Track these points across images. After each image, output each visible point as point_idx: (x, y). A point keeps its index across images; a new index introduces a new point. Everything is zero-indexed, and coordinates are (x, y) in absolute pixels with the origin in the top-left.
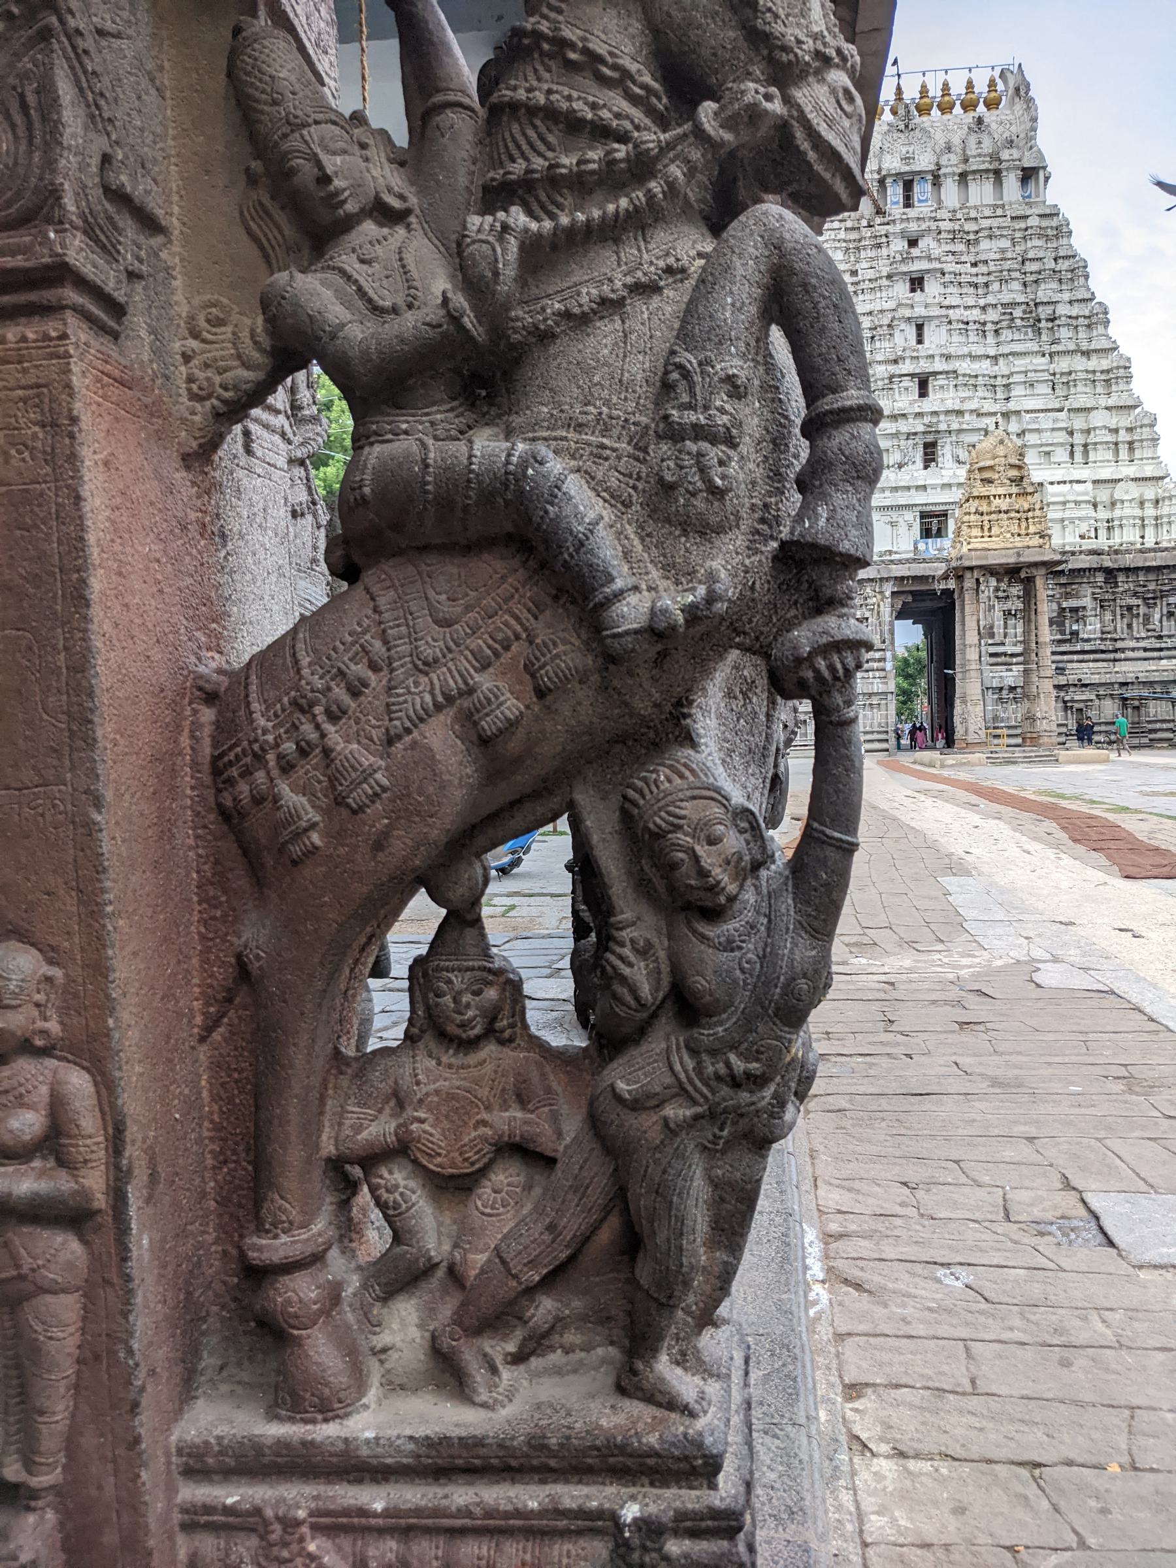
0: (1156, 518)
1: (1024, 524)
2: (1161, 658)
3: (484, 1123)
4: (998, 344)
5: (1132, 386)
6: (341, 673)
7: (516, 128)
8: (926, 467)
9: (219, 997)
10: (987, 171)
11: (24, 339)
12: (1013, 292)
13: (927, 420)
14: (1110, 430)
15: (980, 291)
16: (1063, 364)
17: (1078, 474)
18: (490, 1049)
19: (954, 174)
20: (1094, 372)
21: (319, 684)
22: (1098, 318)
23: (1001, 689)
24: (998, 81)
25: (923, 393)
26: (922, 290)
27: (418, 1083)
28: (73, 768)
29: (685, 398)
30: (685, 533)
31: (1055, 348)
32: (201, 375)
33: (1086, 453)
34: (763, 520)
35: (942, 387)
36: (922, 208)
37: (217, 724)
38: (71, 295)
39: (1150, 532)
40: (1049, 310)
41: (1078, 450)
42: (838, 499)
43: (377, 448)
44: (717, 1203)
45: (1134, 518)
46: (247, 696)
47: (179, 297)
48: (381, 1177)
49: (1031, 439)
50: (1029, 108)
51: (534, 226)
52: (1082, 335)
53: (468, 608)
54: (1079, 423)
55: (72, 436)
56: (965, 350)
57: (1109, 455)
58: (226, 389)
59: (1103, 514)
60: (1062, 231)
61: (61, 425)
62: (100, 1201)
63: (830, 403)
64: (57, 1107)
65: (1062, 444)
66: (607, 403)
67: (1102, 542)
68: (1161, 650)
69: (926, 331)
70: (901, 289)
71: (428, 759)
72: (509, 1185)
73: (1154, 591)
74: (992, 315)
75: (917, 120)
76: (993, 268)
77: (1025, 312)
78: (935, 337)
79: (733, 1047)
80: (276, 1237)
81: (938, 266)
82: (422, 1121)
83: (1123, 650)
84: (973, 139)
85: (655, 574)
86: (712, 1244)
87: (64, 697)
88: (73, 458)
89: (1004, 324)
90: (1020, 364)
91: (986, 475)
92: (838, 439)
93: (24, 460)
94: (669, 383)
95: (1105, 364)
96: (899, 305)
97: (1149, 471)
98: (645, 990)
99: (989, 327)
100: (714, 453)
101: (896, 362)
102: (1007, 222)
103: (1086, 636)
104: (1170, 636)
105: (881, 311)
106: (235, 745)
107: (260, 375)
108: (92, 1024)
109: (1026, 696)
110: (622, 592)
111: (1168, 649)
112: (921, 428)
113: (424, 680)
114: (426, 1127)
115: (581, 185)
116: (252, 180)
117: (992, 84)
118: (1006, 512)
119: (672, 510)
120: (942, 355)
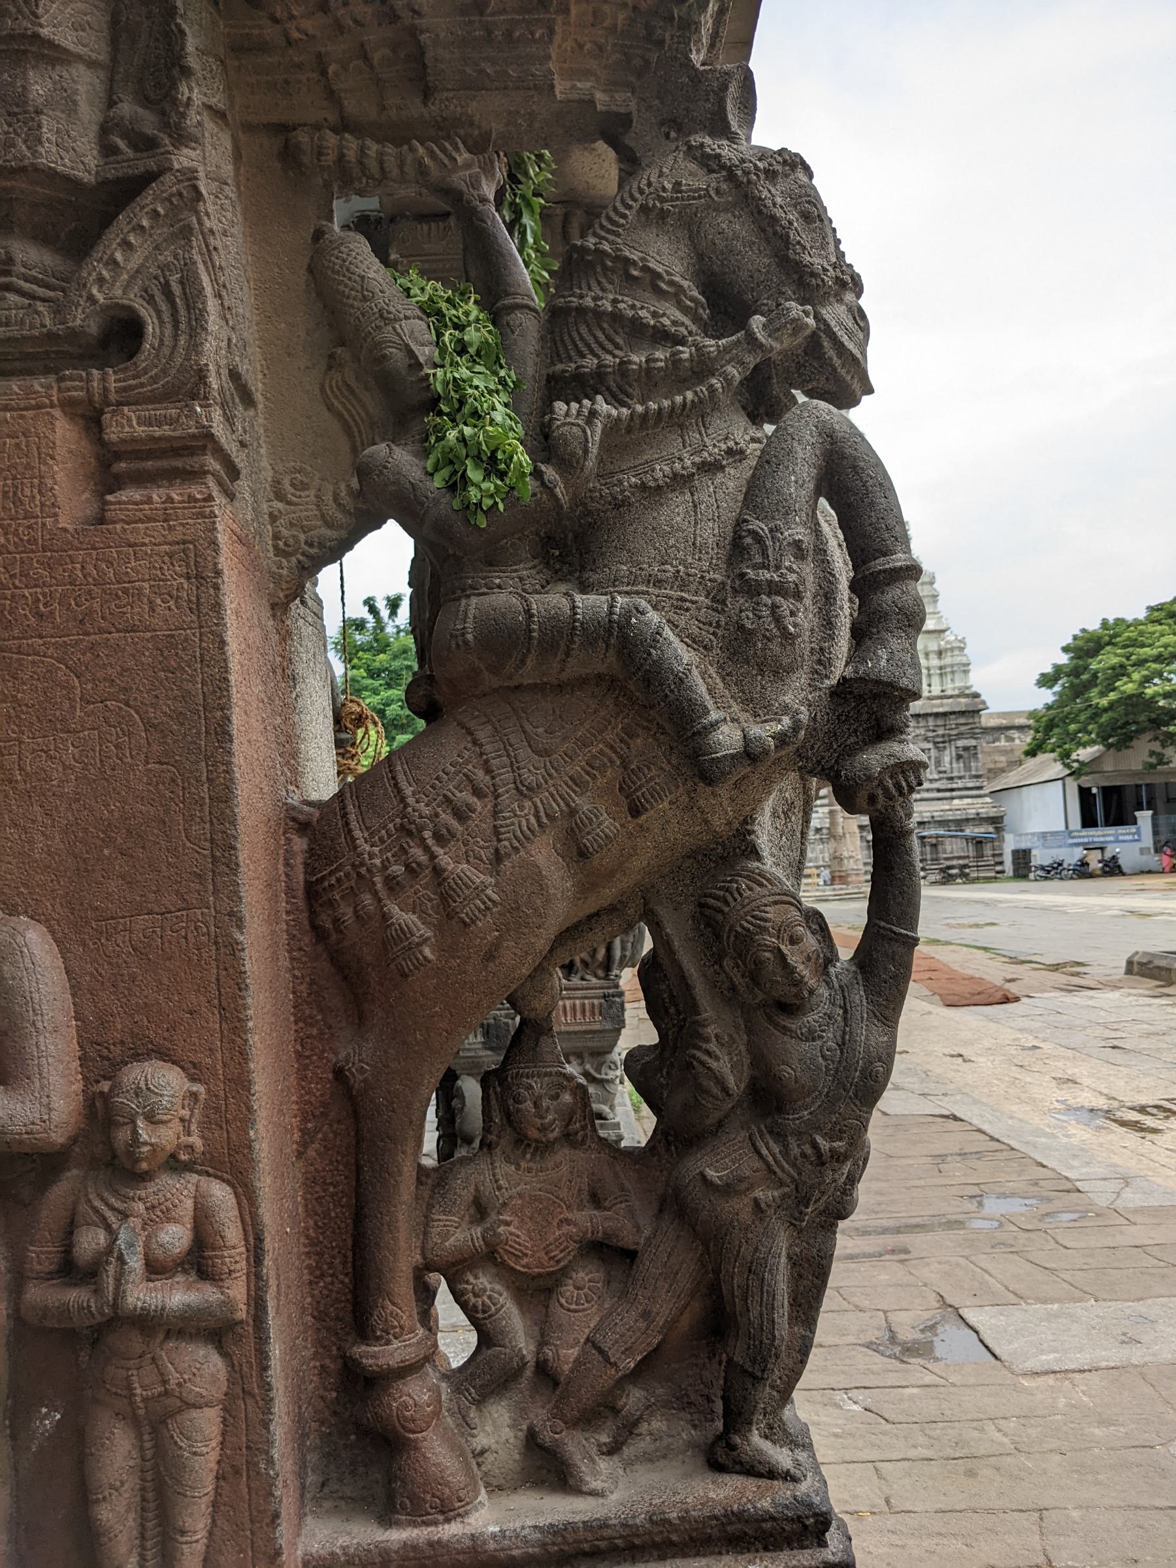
0: (941, 668)
2: (952, 798)
3: (567, 1221)
6: (448, 800)
7: (584, 330)
9: (317, 1113)
11: (170, 500)
18: (564, 1154)
21: (427, 811)
27: (499, 1188)
28: (216, 892)
29: (758, 559)
30: (761, 672)
32: (285, 532)
34: (819, 662)
37: (311, 851)
38: (213, 464)
42: (895, 644)
43: (474, 600)
44: (796, 1278)
46: (347, 824)
47: (265, 463)
48: (467, 1282)
51: (614, 412)
53: (565, 739)
55: (217, 587)
58: (311, 545)
61: (205, 577)
62: (242, 1314)
63: (880, 564)
64: (202, 1221)
66: (683, 562)
68: (952, 790)
71: (536, 876)
72: (590, 1281)
73: (943, 736)
79: (819, 1129)
80: (388, 1342)
82: (508, 1224)
85: (736, 708)
86: (793, 1320)
87: (208, 826)
88: (217, 607)
92: (892, 595)
93: (169, 609)
94: (739, 546)
98: (731, 1081)
100: (785, 605)
104: (960, 778)
106: (337, 869)
107: (344, 534)
108: (233, 1136)
110: (717, 722)
113: (527, 804)
114: (512, 1229)
115: (650, 379)
116: (332, 363)
119: (747, 654)
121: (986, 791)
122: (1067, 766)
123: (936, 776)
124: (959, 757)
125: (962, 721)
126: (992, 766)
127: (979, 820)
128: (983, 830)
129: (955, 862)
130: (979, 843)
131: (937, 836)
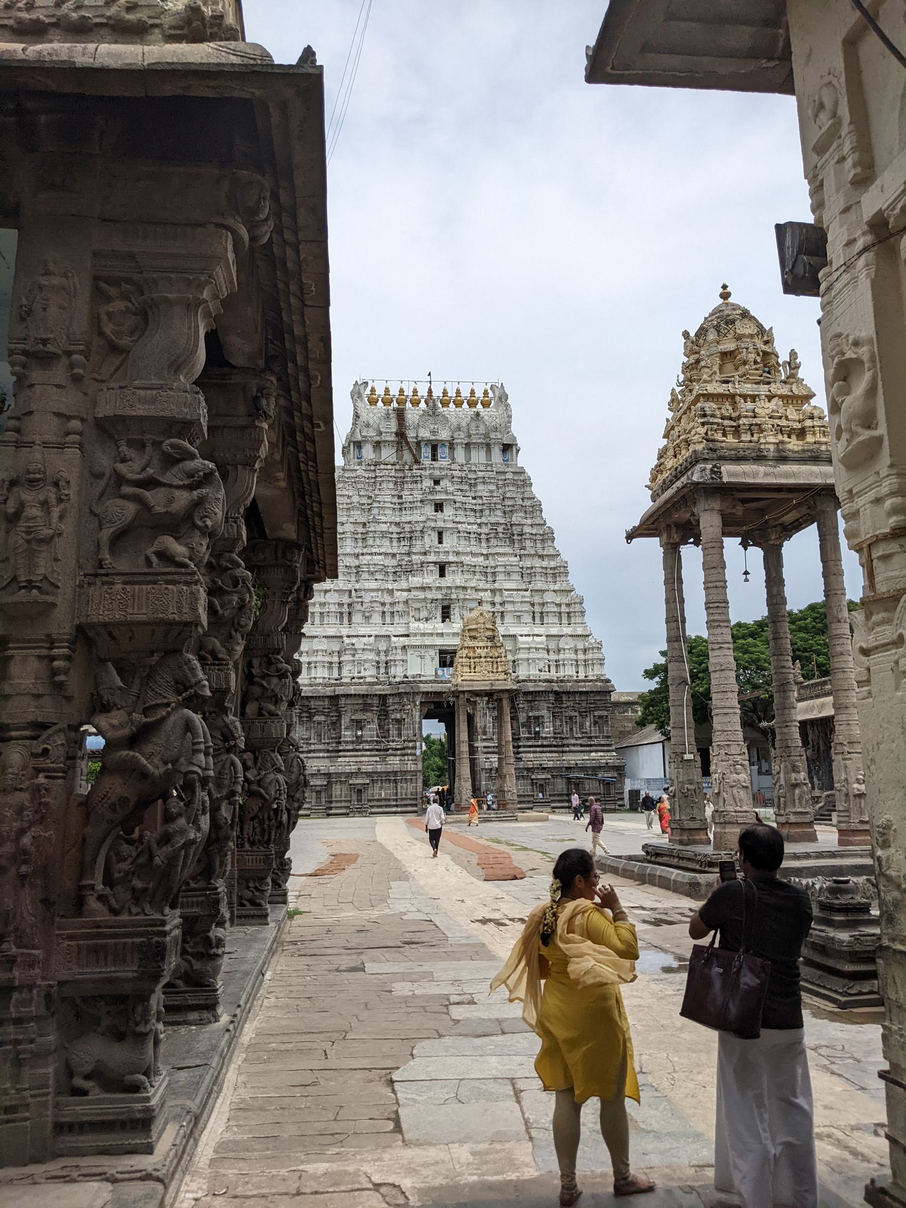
0: (585, 661)
1: (495, 666)
4: (488, 547)
5: (568, 578)
8: (443, 621)
10: (482, 443)
12: (498, 517)
14: (556, 605)
15: (478, 515)
16: (528, 563)
17: (537, 630)
19: (462, 444)
20: (546, 568)
22: (548, 537)
23: (491, 770)
24: (490, 391)
25: (442, 574)
31: (522, 552)
33: (542, 618)
35: (454, 571)
36: (443, 462)
39: (581, 669)
40: (519, 529)
41: (537, 616)
49: (509, 607)
50: (507, 409)
52: (539, 545)
54: (537, 599)
56: (469, 550)
57: (556, 620)
59: (553, 657)
60: (526, 483)
65: (527, 612)
67: (553, 675)
68: (591, 746)
70: (429, 510)
74: (485, 530)
76: (485, 502)
77: (504, 529)
78: (450, 541)
83: (568, 745)
84: (473, 425)
89: (492, 535)
90: (502, 560)
91: (473, 634)
95: (553, 564)
96: (428, 519)
97: (580, 631)
99: (483, 536)
101: (425, 554)
103: (544, 735)
104: (596, 737)
105: (416, 522)
109: (500, 776)
111: (595, 745)
112: (440, 597)
117: (486, 393)
118: (485, 657)
121: (614, 747)
124: (596, 723)
125: (598, 698)
127: (607, 767)
128: (610, 775)
130: (607, 784)
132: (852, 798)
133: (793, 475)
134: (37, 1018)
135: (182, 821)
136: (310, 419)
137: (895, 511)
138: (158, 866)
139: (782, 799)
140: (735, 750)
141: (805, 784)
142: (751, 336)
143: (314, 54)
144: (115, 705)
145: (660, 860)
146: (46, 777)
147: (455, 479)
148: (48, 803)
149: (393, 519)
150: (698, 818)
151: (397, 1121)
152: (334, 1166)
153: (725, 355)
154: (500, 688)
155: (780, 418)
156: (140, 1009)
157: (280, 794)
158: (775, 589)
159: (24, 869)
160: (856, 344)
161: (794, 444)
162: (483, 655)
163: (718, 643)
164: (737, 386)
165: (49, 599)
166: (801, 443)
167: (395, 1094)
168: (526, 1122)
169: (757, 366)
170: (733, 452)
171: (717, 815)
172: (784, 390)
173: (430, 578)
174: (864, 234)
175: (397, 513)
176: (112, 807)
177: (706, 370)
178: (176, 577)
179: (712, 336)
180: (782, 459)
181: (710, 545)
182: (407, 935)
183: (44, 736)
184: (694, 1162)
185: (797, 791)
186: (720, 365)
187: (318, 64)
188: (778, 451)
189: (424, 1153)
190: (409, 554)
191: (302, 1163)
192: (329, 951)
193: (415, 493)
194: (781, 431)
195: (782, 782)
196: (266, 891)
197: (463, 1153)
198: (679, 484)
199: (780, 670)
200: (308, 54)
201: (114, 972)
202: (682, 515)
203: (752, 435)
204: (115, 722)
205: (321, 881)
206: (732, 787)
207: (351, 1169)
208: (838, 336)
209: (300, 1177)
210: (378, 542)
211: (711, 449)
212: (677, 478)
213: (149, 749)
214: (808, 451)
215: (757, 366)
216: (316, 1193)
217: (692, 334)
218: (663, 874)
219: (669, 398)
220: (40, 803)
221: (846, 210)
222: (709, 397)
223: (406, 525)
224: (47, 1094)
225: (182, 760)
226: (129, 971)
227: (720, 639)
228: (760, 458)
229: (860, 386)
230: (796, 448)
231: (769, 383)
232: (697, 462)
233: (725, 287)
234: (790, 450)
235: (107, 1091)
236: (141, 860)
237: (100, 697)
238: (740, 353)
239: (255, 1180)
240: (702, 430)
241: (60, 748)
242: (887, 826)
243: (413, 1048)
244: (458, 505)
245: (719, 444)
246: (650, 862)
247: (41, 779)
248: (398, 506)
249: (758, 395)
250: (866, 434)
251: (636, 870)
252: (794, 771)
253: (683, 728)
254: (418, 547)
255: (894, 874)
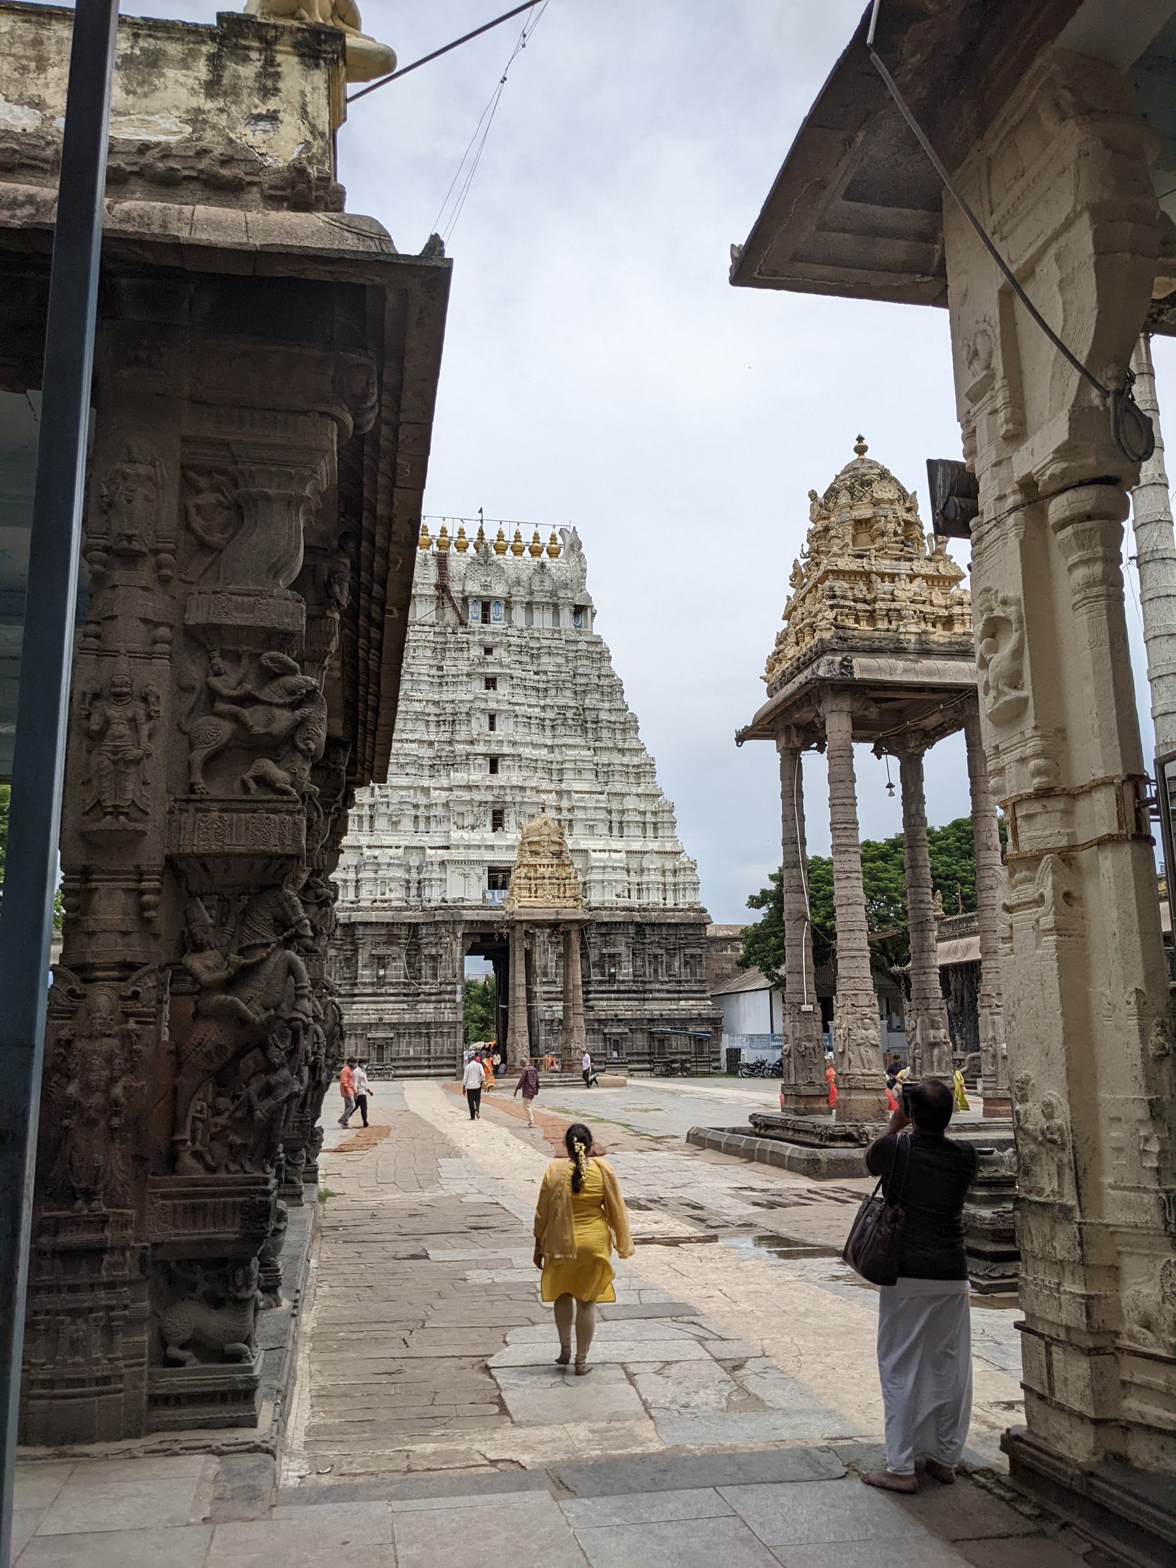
0: (675, 885)
1: (562, 890)
4: (554, 736)
8: (494, 830)
10: (548, 603)
13: (495, 792)
15: (541, 694)
16: (604, 758)
20: (628, 766)
22: (630, 726)
23: (552, 1021)
25: (494, 770)
26: (495, 689)
31: (598, 744)
33: (621, 829)
35: (509, 767)
36: (497, 625)
39: (670, 895)
40: (593, 714)
41: (615, 826)
45: (658, 883)
50: (580, 561)
56: (528, 739)
57: (639, 832)
59: (634, 879)
60: (603, 656)
65: (603, 821)
67: (634, 901)
68: (680, 992)
69: (498, 721)
70: (478, 687)
74: (550, 714)
75: (496, 557)
76: (551, 678)
77: (575, 714)
78: (504, 728)
81: (508, 671)
83: (651, 991)
84: (537, 579)
89: (559, 722)
91: (534, 848)
95: (636, 761)
96: (476, 698)
97: (668, 847)
99: (547, 722)
101: (472, 743)
102: (562, 644)
104: (687, 982)
105: (461, 701)
109: (565, 1029)
111: (685, 992)
112: (491, 799)
117: (553, 538)
120: (509, 741)
121: (708, 994)
122: (772, 980)
123: (666, 979)
124: (687, 963)
126: (719, 972)
127: (700, 1019)
128: (703, 1029)
129: (679, 1057)
130: (699, 1040)
131: (663, 1033)
132: (1000, 1059)
133: (938, 672)
134: (131, 1283)
135: (285, 1072)
136: (382, 604)
137: (1038, 772)
138: (260, 1120)
139: (918, 1061)
140: (863, 1000)
141: (946, 1043)
142: (891, 502)
143: (442, 244)
144: (209, 944)
145: (771, 1132)
146: (137, 1022)
147: (512, 648)
148: (140, 1052)
149: (430, 696)
150: (817, 1082)
151: (501, 1403)
152: (443, 1446)
153: (859, 523)
154: (567, 917)
155: (924, 602)
156: (240, 1273)
157: (319, 1048)
158: (913, 807)
159: (116, 1121)
160: (1004, 602)
161: (939, 635)
162: (547, 875)
163: (846, 872)
164: (873, 562)
165: (139, 826)
166: (947, 633)
167: (495, 1380)
168: (644, 1403)
169: (897, 539)
170: (866, 643)
171: (841, 1078)
172: (929, 570)
173: (478, 774)
174: (1014, 492)
175: (436, 689)
176: (208, 1057)
177: (837, 541)
178: (279, 805)
179: (844, 499)
180: (925, 651)
181: (837, 753)
182: (472, 1219)
183: (134, 979)
184: (826, 1435)
185: (936, 1052)
186: (854, 536)
187: (447, 256)
188: (920, 642)
189: (538, 1432)
190: (450, 743)
191: (406, 1444)
192: (379, 1237)
193: (460, 663)
194: (925, 618)
195: (918, 1039)
196: (300, 1165)
197: (581, 1431)
198: (801, 678)
199: (918, 906)
200: (435, 244)
201: (214, 1233)
202: (806, 715)
203: (890, 622)
204: (210, 963)
205: (350, 1158)
206: (858, 1045)
207: (462, 1447)
208: (988, 590)
209: (408, 1457)
210: (410, 726)
211: (840, 638)
212: (799, 670)
213: (248, 992)
214: (956, 643)
215: (897, 539)
216: (429, 1470)
217: (820, 495)
218: (776, 1150)
219: (791, 571)
220: (131, 1052)
221: (998, 464)
222: (839, 574)
223: (447, 705)
224: (141, 1364)
225: (284, 1005)
226: (229, 1232)
227: (847, 868)
228: (898, 650)
229: (1008, 645)
230: (942, 640)
231: (911, 560)
232: (824, 652)
233: (860, 439)
234: (934, 642)
235: (203, 1362)
236: (239, 1114)
237: (192, 935)
238: (878, 522)
239: (359, 1460)
240: (831, 615)
241: (152, 991)
242: (1026, 1082)
243: (505, 1336)
244: (515, 681)
245: (850, 633)
246: (758, 1135)
247: (132, 1025)
248: (436, 680)
249: (898, 574)
250: (1013, 694)
251: (742, 1145)
252: (933, 1027)
253: (801, 973)
254: (462, 733)
255: (1031, 1127)
